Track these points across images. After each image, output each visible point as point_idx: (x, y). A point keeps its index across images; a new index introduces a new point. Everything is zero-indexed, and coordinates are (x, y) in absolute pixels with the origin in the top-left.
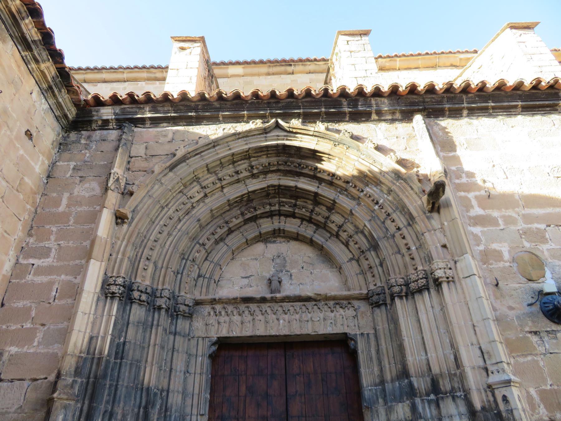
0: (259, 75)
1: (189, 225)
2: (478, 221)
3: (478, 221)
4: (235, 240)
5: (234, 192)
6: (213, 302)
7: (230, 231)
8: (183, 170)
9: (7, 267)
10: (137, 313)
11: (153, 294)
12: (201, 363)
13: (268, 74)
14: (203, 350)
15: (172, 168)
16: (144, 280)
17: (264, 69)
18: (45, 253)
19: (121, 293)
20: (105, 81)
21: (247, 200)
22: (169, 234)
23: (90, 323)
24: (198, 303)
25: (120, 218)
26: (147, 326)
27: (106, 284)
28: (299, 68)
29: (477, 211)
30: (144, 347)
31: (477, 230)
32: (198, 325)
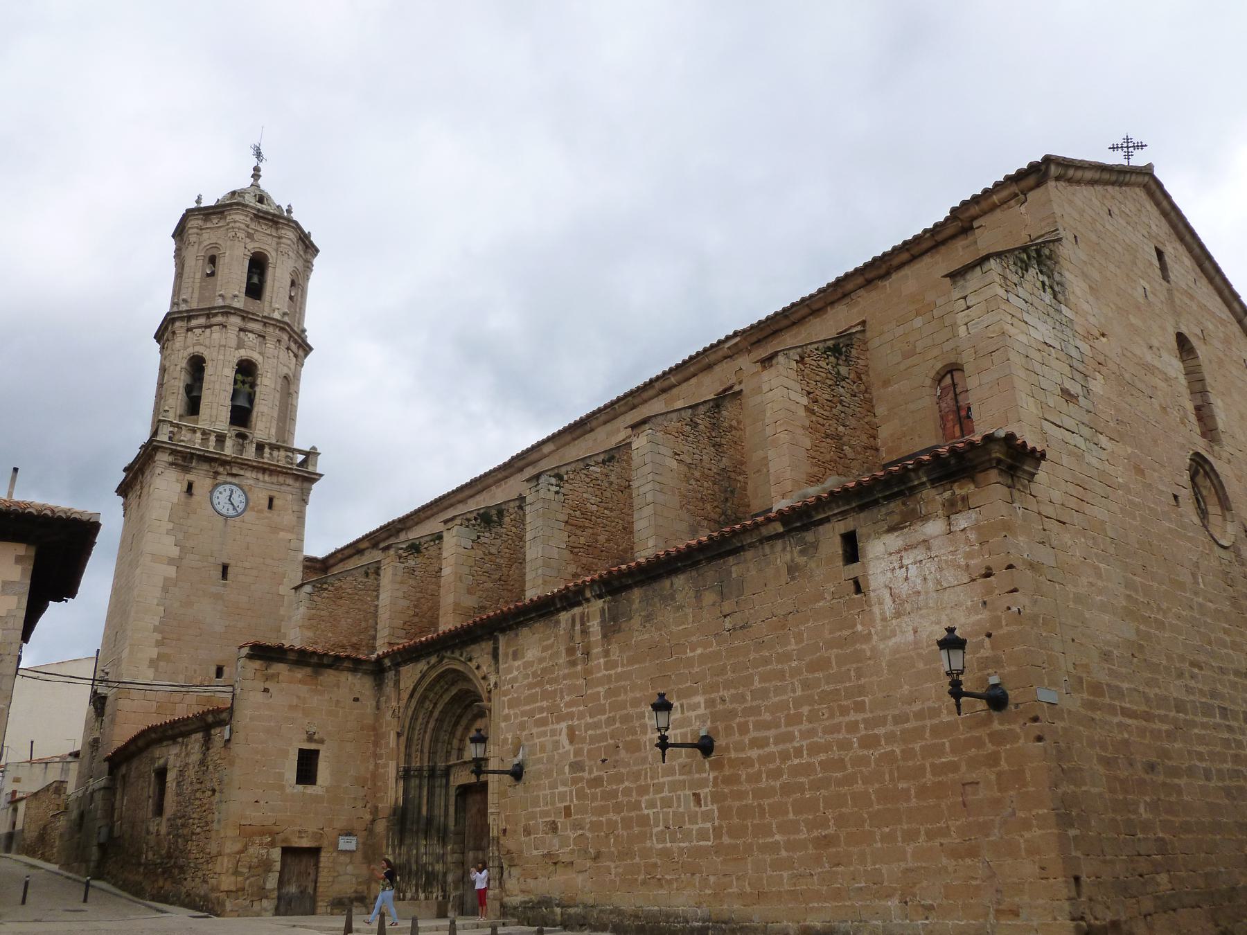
0: (568, 443)
1: (431, 725)
2: (507, 718)
3: (507, 718)
4: (464, 722)
5: (446, 698)
6: (455, 765)
7: (460, 717)
8: (417, 695)
9: (371, 767)
10: (414, 782)
11: (421, 769)
12: (452, 800)
13: (574, 439)
14: (452, 792)
15: (411, 696)
16: (416, 764)
17: (568, 438)
18: (380, 757)
19: (406, 775)
20: (471, 497)
21: (454, 700)
22: (425, 732)
23: (392, 793)
24: (448, 768)
25: (399, 735)
26: (420, 787)
27: (398, 772)
28: (594, 423)
29: (506, 711)
30: (420, 797)
31: (503, 725)
32: (452, 778)
